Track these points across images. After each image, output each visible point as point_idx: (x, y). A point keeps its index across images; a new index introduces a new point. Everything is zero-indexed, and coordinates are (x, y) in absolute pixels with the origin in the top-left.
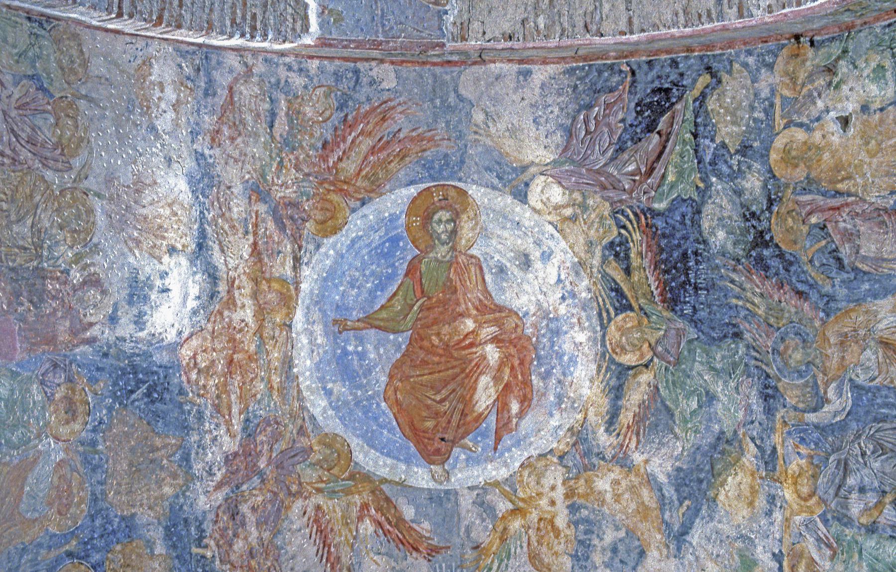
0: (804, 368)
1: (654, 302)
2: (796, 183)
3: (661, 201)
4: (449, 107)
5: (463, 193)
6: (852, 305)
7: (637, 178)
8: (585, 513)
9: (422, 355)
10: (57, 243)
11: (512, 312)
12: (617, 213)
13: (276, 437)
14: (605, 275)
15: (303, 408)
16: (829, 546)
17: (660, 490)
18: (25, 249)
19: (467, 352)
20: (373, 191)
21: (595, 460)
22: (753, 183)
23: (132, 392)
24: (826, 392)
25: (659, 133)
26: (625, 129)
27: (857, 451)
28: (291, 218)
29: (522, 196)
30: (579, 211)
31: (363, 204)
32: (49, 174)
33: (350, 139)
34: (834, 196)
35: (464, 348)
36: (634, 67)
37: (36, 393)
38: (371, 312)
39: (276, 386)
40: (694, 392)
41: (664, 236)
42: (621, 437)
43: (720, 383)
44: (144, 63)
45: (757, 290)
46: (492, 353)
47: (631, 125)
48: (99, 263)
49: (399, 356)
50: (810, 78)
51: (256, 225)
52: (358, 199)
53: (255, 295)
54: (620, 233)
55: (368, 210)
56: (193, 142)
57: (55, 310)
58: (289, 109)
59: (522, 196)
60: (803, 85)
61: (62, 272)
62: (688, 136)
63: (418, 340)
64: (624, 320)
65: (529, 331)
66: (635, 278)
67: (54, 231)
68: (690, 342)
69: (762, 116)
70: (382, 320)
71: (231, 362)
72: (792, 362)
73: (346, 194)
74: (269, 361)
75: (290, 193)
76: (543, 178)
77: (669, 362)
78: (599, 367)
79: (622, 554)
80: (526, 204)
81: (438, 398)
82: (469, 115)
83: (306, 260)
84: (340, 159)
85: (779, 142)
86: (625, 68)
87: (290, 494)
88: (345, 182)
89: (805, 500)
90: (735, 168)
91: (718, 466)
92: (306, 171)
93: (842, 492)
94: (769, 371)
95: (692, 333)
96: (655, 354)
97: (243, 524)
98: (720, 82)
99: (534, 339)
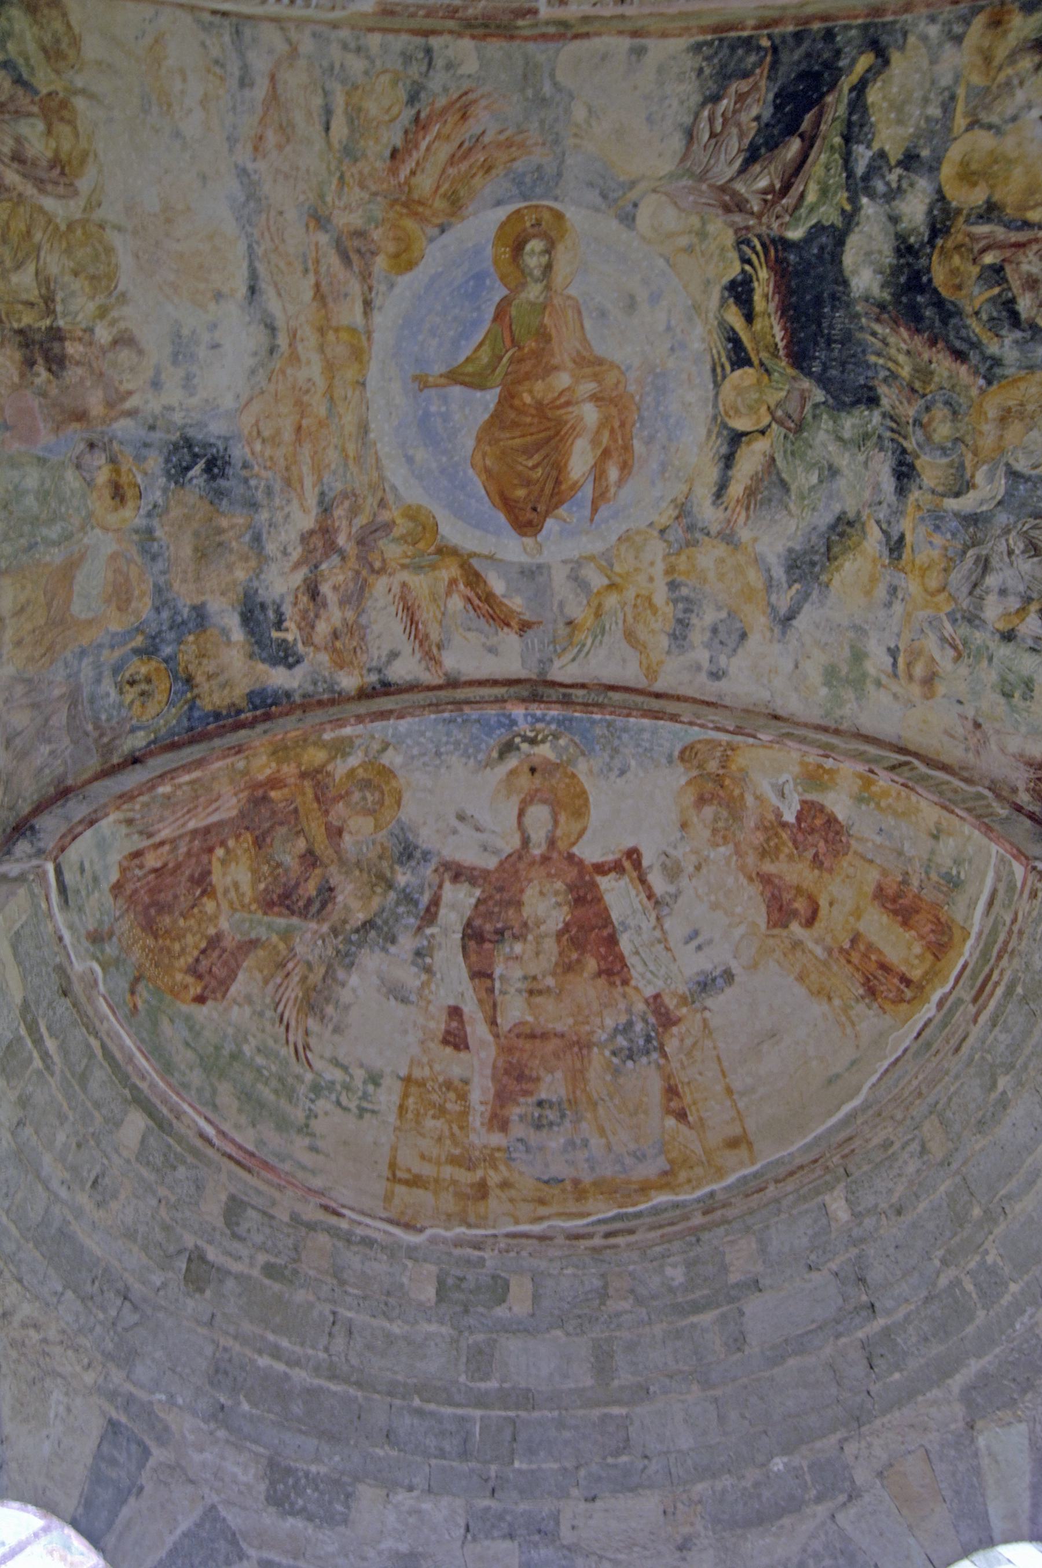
0: (949, 445)
1: (777, 357)
3: (796, 228)
4: (544, 100)
5: (559, 216)
6: (1023, 373)
8: (684, 591)
9: (512, 415)
10: (73, 294)
11: (613, 365)
13: (354, 511)
14: (722, 323)
15: (382, 478)
16: (954, 647)
17: (769, 570)
18: (32, 305)
20: (453, 214)
21: (698, 535)
22: (915, 209)
23: (188, 469)
24: (973, 476)
25: (801, 136)
26: (759, 131)
27: (1003, 547)
28: (359, 251)
29: (628, 219)
30: (695, 240)
31: (443, 231)
32: (49, 203)
33: (423, 145)
34: (1019, 229)
35: (559, 407)
36: (777, 41)
37: (72, 479)
38: (455, 364)
39: (351, 454)
41: (797, 274)
43: (847, 455)
44: (156, 41)
45: (903, 346)
46: (590, 414)
47: (767, 125)
48: (130, 317)
49: (486, 416)
50: (1012, 58)
51: (317, 262)
53: (321, 349)
54: (743, 271)
56: (231, 150)
57: (82, 380)
58: (347, 104)
59: (628, 219)
60: (1000, 68)
61: (85, 331)
62: (837, 140)
63: (508, 398)
64: (741, 378)
65: (632, 388)
66: (758, 325)
67: (66, 278)
68: (816, 406)
70: (468, 375)
71: (299, 428)
72: (936, 438)
73: (423, 220)
74: (342, 427)
75: (354, 220)
76: (654, 197)
78: (709, 432)
79: (722, 635)
81: (530, 464)
82: (567, 111)
83: (377, 303)
85: (955, 153)
86: (765, 43)
87: (373, 571)
89: (932, 595)
90: (894, 185)
91: (836, 550)
92: (373, 188)
93: (978, 592)
94: (905, 444)
96: (774, 419)
97: (325, 605)
98: (886, 62)
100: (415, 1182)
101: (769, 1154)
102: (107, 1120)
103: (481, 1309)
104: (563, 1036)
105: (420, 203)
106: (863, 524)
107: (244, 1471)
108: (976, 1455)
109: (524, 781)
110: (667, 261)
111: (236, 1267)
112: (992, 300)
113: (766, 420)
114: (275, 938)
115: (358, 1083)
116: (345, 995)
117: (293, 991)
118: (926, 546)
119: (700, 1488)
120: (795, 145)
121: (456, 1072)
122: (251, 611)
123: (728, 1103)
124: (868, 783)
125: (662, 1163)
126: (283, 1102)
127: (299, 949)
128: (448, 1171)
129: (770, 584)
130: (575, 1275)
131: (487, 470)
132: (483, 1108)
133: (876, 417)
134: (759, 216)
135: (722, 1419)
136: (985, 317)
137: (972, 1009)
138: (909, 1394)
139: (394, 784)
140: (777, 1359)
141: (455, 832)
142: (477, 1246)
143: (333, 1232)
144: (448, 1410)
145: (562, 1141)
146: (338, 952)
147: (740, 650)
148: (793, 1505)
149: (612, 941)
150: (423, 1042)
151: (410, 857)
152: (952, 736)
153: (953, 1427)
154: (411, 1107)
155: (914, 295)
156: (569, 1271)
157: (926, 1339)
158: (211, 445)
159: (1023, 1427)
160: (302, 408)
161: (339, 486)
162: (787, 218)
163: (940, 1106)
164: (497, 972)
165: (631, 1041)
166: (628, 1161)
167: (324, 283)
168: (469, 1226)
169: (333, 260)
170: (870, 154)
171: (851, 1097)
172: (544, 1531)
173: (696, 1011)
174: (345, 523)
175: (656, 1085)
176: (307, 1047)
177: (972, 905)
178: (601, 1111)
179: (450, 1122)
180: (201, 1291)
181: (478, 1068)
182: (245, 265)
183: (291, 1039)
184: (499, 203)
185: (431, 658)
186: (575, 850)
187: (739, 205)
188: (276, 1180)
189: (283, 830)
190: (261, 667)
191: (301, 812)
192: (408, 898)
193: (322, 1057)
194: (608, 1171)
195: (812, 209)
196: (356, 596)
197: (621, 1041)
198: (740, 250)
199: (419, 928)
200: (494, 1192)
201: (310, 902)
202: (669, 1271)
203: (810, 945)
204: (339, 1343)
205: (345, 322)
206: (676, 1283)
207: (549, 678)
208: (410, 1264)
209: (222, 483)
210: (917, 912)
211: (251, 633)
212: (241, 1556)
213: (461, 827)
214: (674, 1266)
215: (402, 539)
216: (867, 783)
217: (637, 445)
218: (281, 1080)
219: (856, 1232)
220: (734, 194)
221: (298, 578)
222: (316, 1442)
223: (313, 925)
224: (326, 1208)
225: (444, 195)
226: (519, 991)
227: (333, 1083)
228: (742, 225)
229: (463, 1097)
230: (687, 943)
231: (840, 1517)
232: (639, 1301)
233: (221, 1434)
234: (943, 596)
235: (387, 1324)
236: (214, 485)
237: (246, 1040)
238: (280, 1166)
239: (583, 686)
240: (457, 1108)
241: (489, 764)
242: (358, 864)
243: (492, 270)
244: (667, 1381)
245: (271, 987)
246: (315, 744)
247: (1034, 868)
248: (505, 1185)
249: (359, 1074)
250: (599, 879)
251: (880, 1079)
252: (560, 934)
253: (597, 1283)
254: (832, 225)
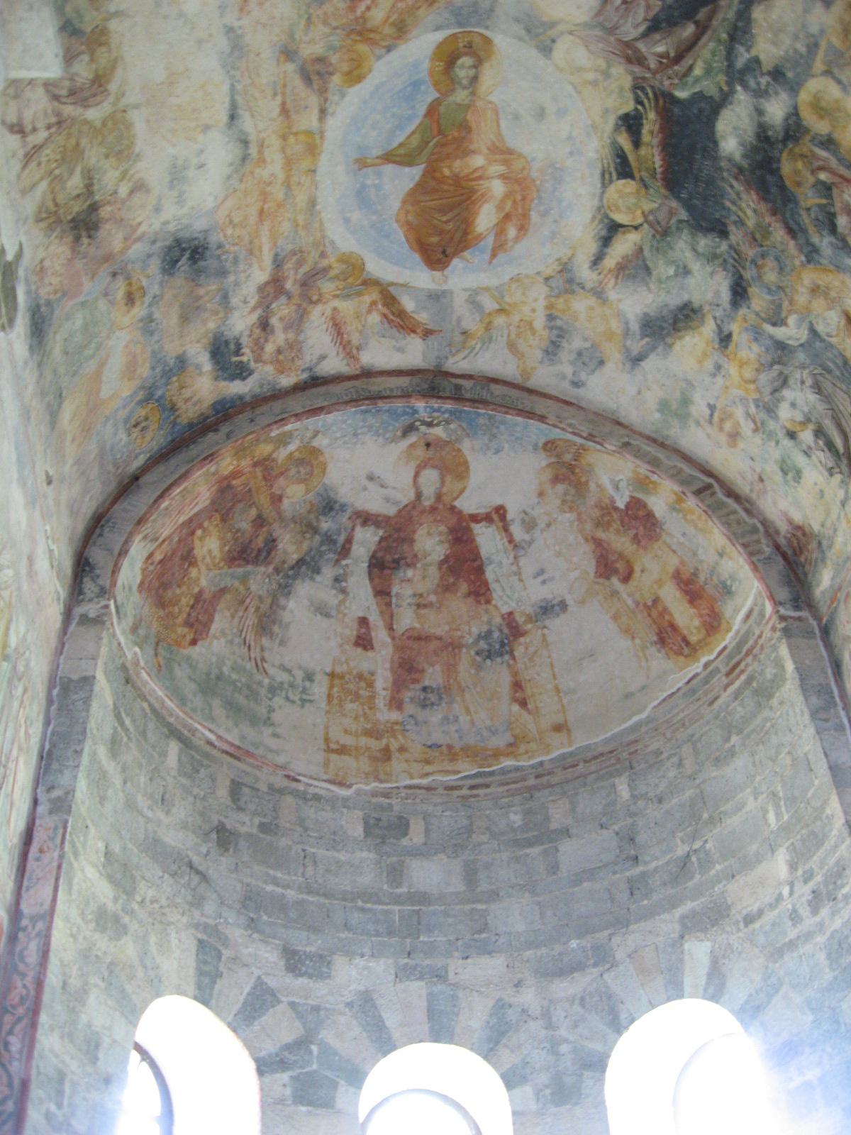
1: (655, 178)
2: (817, 134)
5: (488, 41)
6: (832, 268)
7: (664, 61)
8: (559, 323)
9: (433, 184)
11: (521, 156)
12: (638, 88)
13: (300, 264)
15: (324, 237)
19: (474, 183)
20: (399, 37)
21: (575, 287)
22: (776, 110)
23: (177, 261)
24: (786, 318)
25: (696, 23)
26: (663, 9)
28: (319, 73)
30: (600, 78)
39: (301, 223)
40: (673, 262)
42: (602, 276)
45: (751, 204)
46: (498, 188)
47: (670, 7)
49: (411, 185)
51: (285, 86)
52: (385, 47)
53: (283, 150)
54: (636, 109)
55: (393, 56)
59: (546, 50)
62: (724, 36)
63: (431, 172)
65: (534, 174)
66: (643, 151)
68: (680, 221)
69: (803, 50)
70: (400, 156)
75: (318, 49)
77: (657, 231)
78: (594, 218)
80: (550, 59)
81: (444, 219)
84: (368, 8)
88: (372, 31)
90: (763, 87)
91: (681, 325)
92: (334, 24)
93: (777, 395)
94: (743, 272)
95: (684, 215)
96: (646, 221)
97: (272, 332)
99: (538, 182)
100: (343, 750)
101: (581, 740)
102: (160, 755)
103: (392, 840)
104: (440, 639)
105: (372, 31)
106: (703, 316)
107: (269, 956)
108: (682, 953)
109: (421, 452)
110: (575, 88)
111: (244, 829)
112: (820, 206)
113: (640, 220)
114: (237, 584)
115: (299, 681)
116: (286, 616)
117: (251, 620)
118: (747, 350)
119: (528, 953)
120: (689, 30)
121: (365, 666)
122: (218, 348)
123: (556, 698)
124: (679, 500)
125: (508, 738)
126: (252, 704)
127: (254, 587)
128: (364, 741)
129: (627, 332)
130: (451, 817)
131: (408, 223)
132: (384, 693)
133: (724, 247)
134: (655, 73)
135: (542, 915)
136: (813, 215)
137: (725, 680)
138: (650, 914)
139: (321, 459)
140: (577, 879)
141: (365, 489)
142: (387, 795)
143: (295, 793)
144: (381, 907)
145: (440, 717)
146: (280, 585)
147: (597, 373)
148: (579, 967)
149: (480, 570)
150: (341, 646)
151: (331, 509)
152: (744, 478)
153: (672, 936)
154: (336, 695)
155: (764, 162)
156: (447, 813)
157: (665, 884)
158: (196, 239)
159: (709, 944)
160: (265, 196)
161: (290, 247)
162: (676, 81)
163: (694, 739)
164: (393, 593)
165: (490, 644)
166: (486, 733)
167: (288, 101)
168: (381, 781)
169: (298, 82)
170: (747, 56)
171: (641, 711)
172: (439, 975)
173: (538, 628)
174: (292, 272)
175: (506, 679)
176: (263, 659)
177: (737, 611)
178: (467, 696)
179: (362, 704)
180: (227, 850)
181: (380, 664)
182: (227, 99)
183: (253, 656)
184: (438, 28)
185: (349, 350)
186: (457, 503)
187: (639, 60)
188: (256, 763)
189: (241, 506)
190: (223, 384)
191: (254, 489)
192: (329, 539)
193: (273, 666)
194: (471, 740)
195: (697, 80)
196: (297, 323)
197: (483, 645)
198: (635, 94)
199: (337, 561)
200: (396, 755)
201: (260, 551)
202: (512, 817)
203: (625, 596)
204: (310, 871)
205: (303, 128)
206: (516, 825)
207: (444, 369)
208: (345, 810)
209: (202, 263)
210: (701, 598)
211: (217, 363)
212: (279, 1002)
213: (370, 485)
214: (516, 813)
215: (337, 277)
216: (679, 500)
217: (533, 215)
218: (249, 687)
219: (632, 808)
220: (637, 51)
221: (254, 318)
222: (306, 933)
223: (262, 569)
224: (288, 777)
225: (393, 24)
226: (409, 604)
227: (282, 683)
228: (638, 75)
229: (370, 685)
230: (535, 577)
231: (605, 976)
232: (493, 836)
233: (255, 936)
234: (752, 386)
235: (336, 854)
236: (195, 267)
237: (224, 664)
238: (256, 752)
239: (470, 377)
240: (367, 694)
241: (394, 440)
242: (293, 520)
243: (427, 79)
244: (510, 890)
245: (236, 620)
246: (265, 441)
247: (778, 612)
248: (402, 749)
249: (299, 674)
250: (473, 525)
251: (660, 704)
252: (441, 563)
253: (466, 822)
254: (711, 97)
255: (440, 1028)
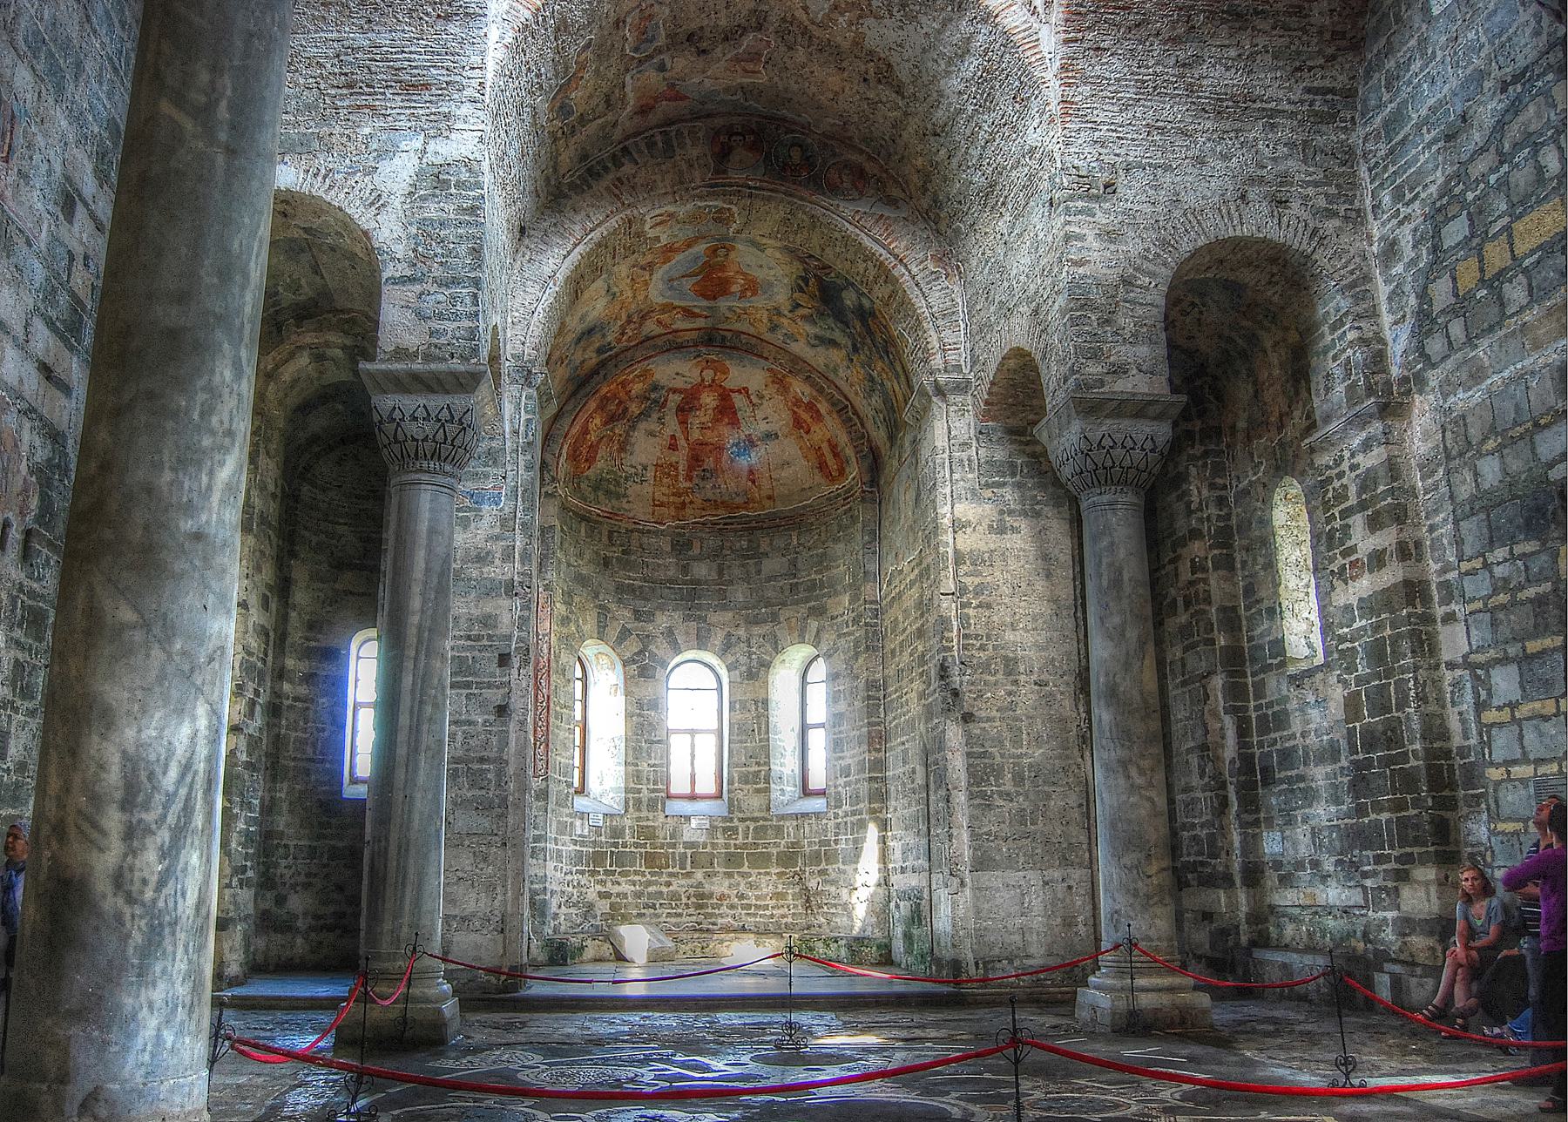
100: (662, 505)
121: (674, 459)
138: (796, 603)
140: (769, 579)
149: (735, 413)
181: (681, 458)
192: (655, 401)
255: (701, 642)
